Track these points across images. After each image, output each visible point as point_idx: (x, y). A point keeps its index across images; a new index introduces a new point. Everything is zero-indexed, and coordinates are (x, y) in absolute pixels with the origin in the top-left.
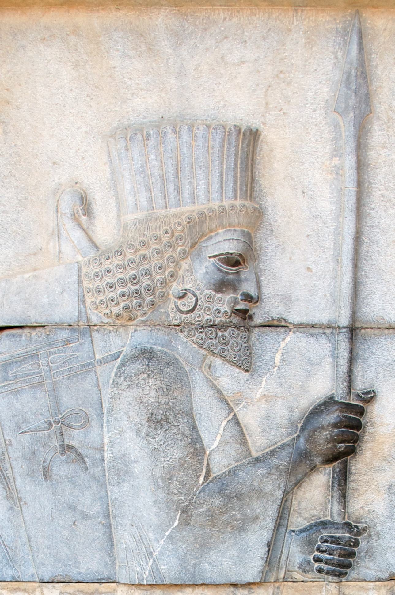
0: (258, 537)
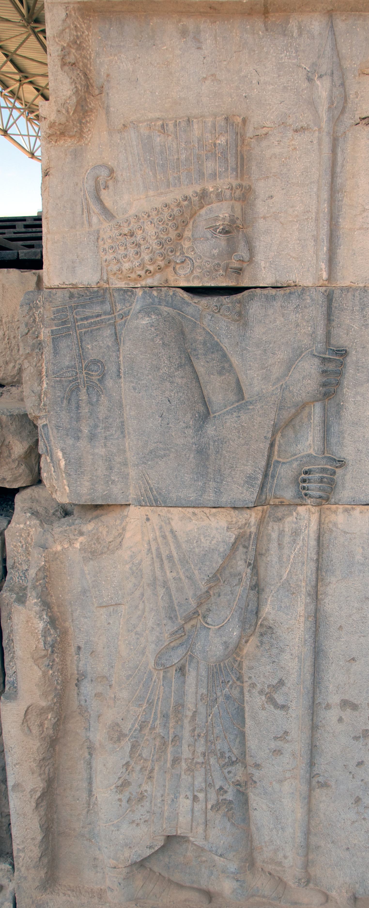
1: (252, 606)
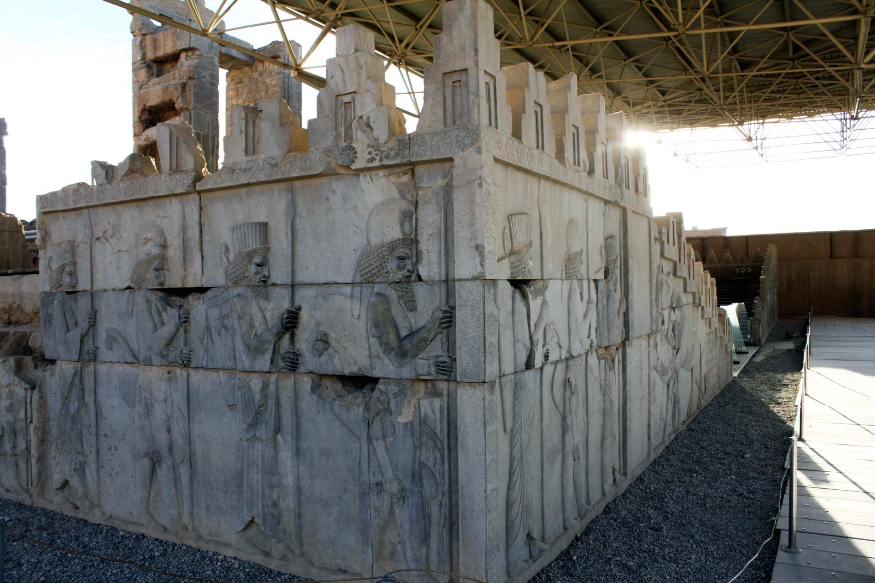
0: (268, 356)
1: (81, 395)
